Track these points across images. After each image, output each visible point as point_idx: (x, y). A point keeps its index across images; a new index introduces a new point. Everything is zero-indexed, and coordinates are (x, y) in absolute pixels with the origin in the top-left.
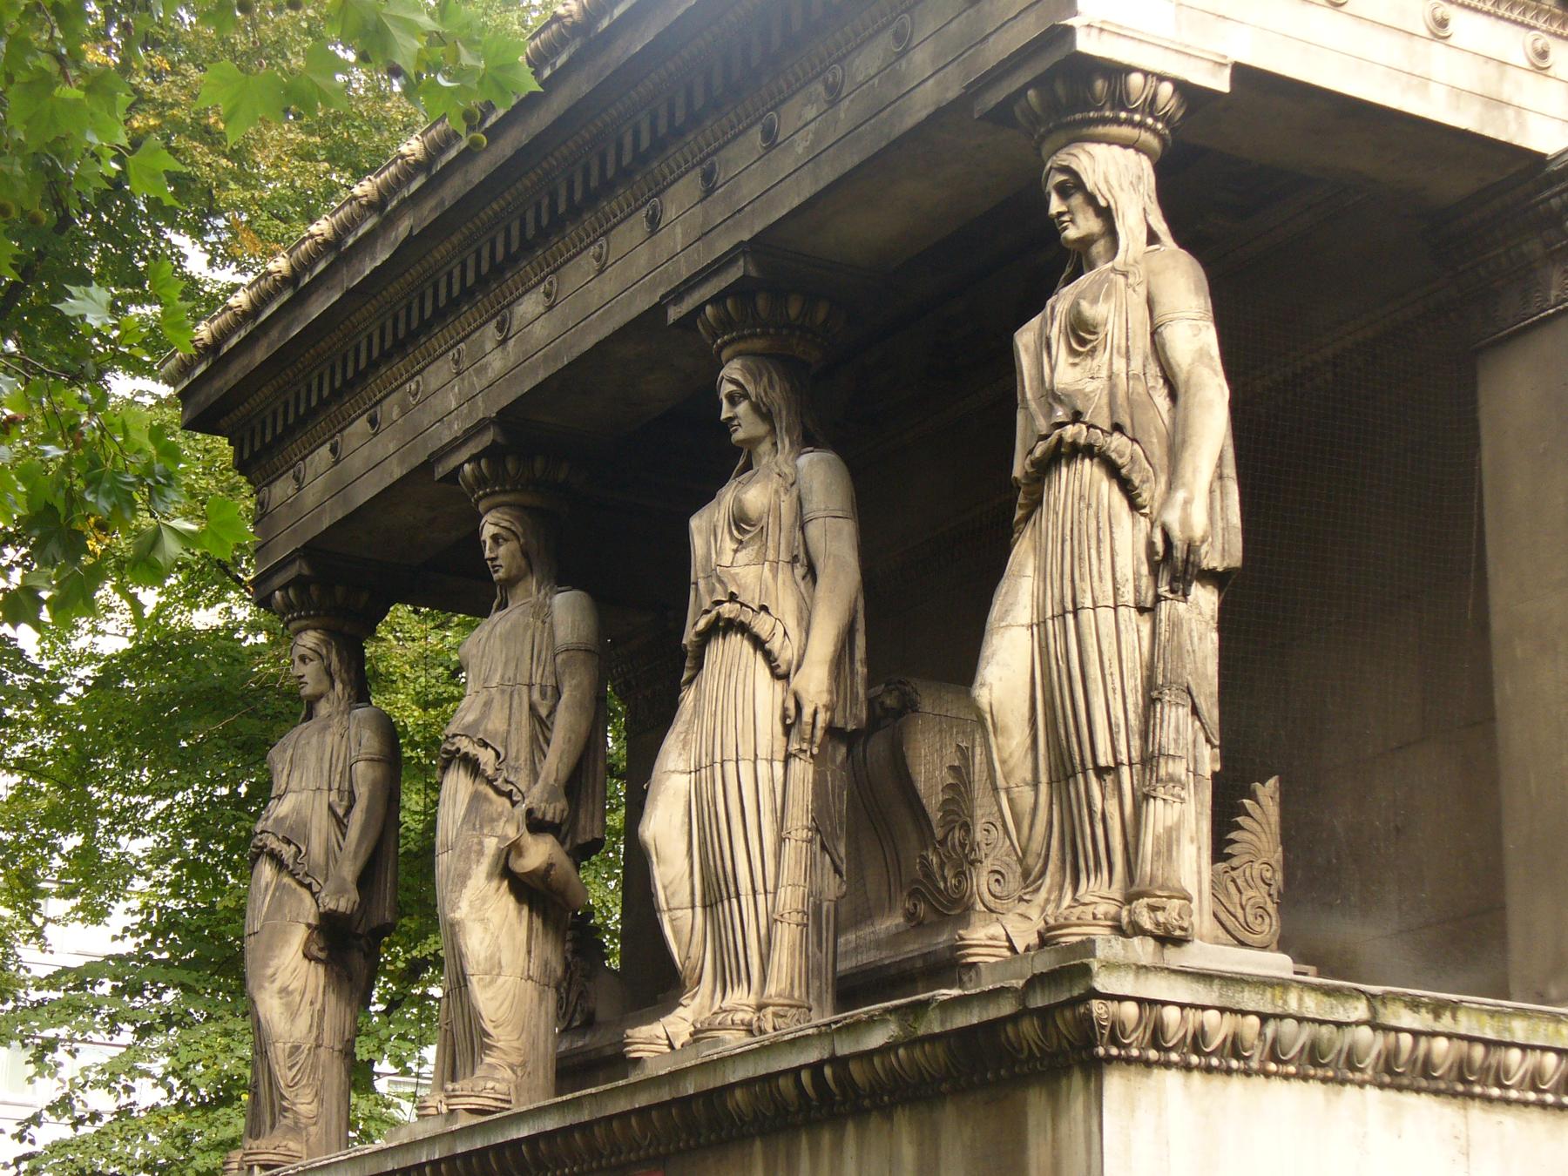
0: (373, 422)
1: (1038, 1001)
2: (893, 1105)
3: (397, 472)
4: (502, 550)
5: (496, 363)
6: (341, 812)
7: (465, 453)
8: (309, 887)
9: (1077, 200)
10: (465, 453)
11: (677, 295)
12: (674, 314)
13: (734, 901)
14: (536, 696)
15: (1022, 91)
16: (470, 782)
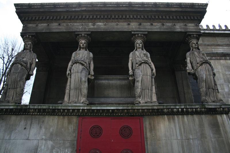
0: (59, 25)
1: (223, 107)
2: (194, 114)
3: (64, 31)
4: (85, 45)
5: (92, 27)
6: (31, 63)
7: (84, 33)
8: (27, 70)
9: (197, 45)
10: (84, 33)
11: (135, 31)
12: (133, 33)
13: (148, 90)
14: (89, 61)
15: (194, 34)
16: (81, 66)
